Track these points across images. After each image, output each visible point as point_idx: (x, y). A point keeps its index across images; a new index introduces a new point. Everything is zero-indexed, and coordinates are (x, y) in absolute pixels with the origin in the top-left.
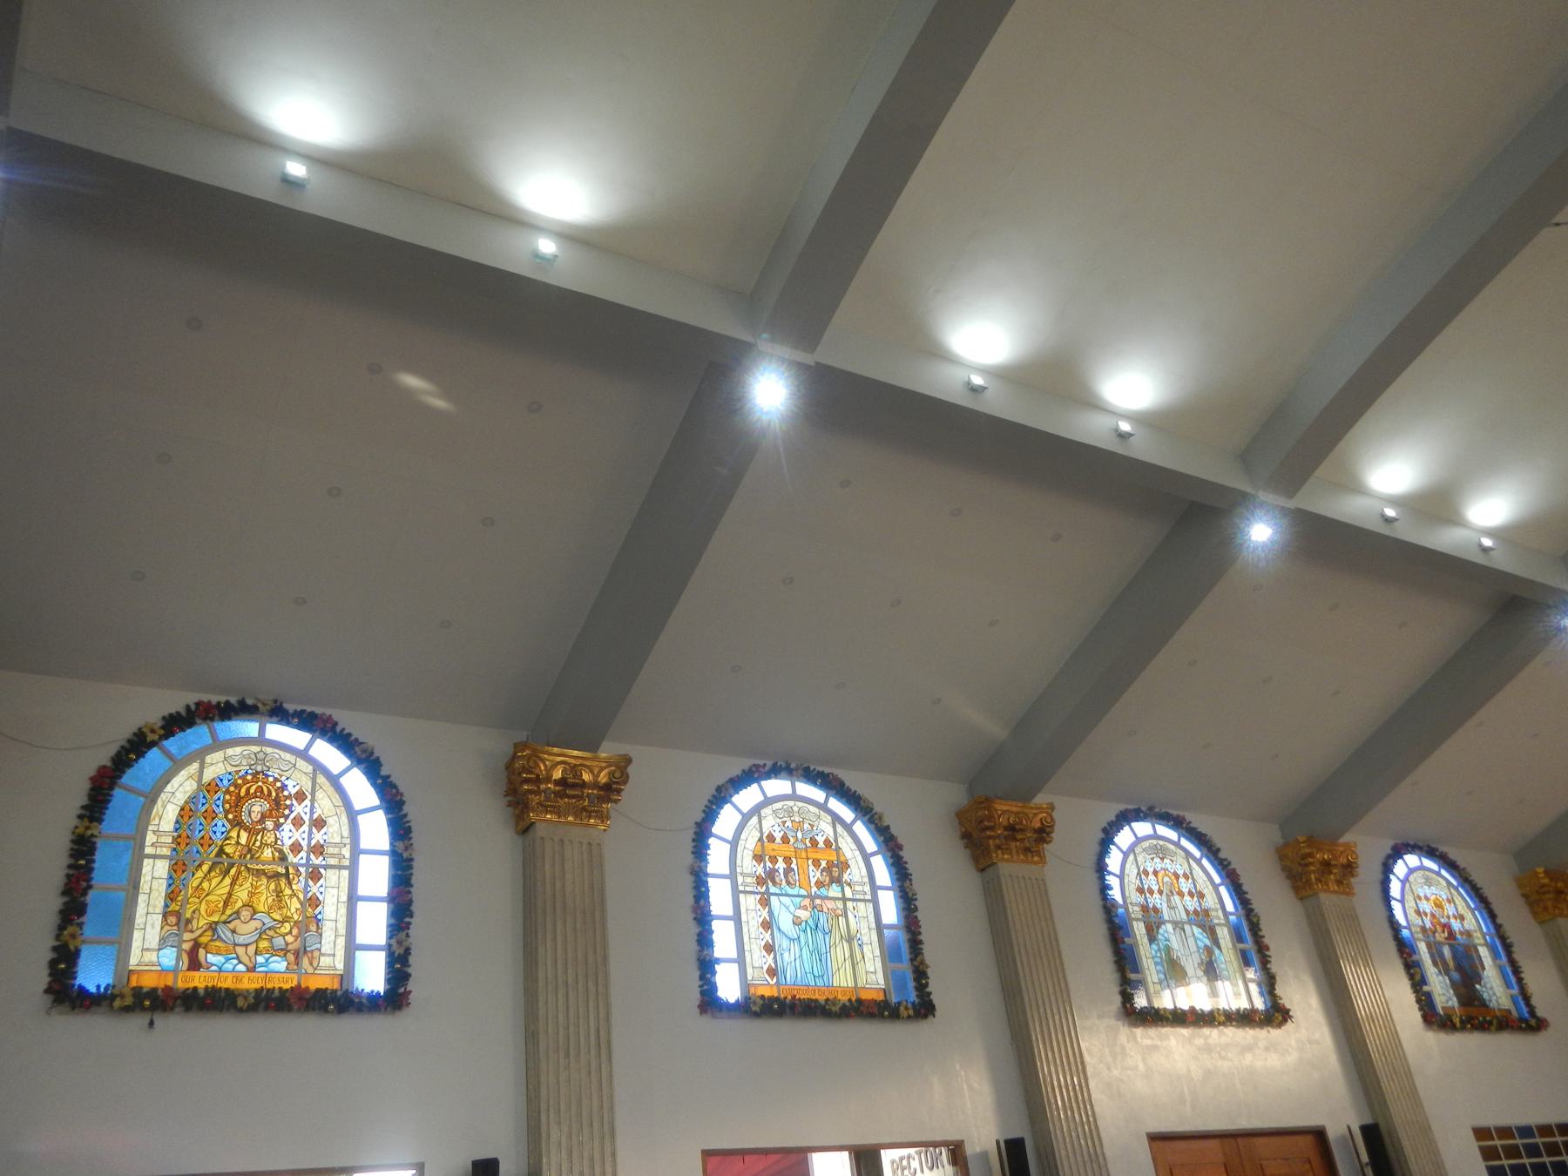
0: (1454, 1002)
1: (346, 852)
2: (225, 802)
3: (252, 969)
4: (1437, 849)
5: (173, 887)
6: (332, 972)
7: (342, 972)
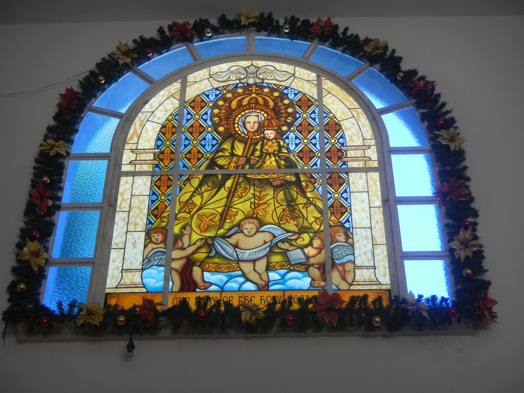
1: (373, 154)
2: (213, 116)
3: (264, 287)
5: (157, 204)
6: (375, 287)
7: (389, 287)
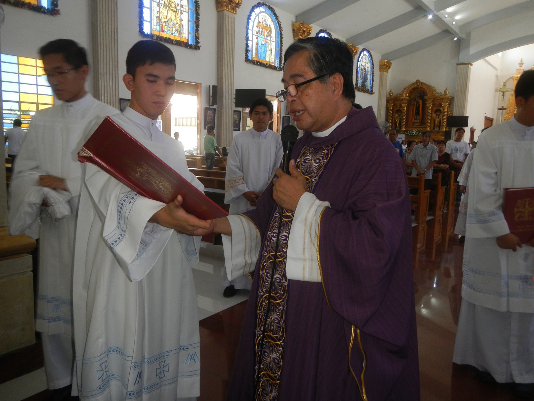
0: (361, 86)
4: (370, 51)
